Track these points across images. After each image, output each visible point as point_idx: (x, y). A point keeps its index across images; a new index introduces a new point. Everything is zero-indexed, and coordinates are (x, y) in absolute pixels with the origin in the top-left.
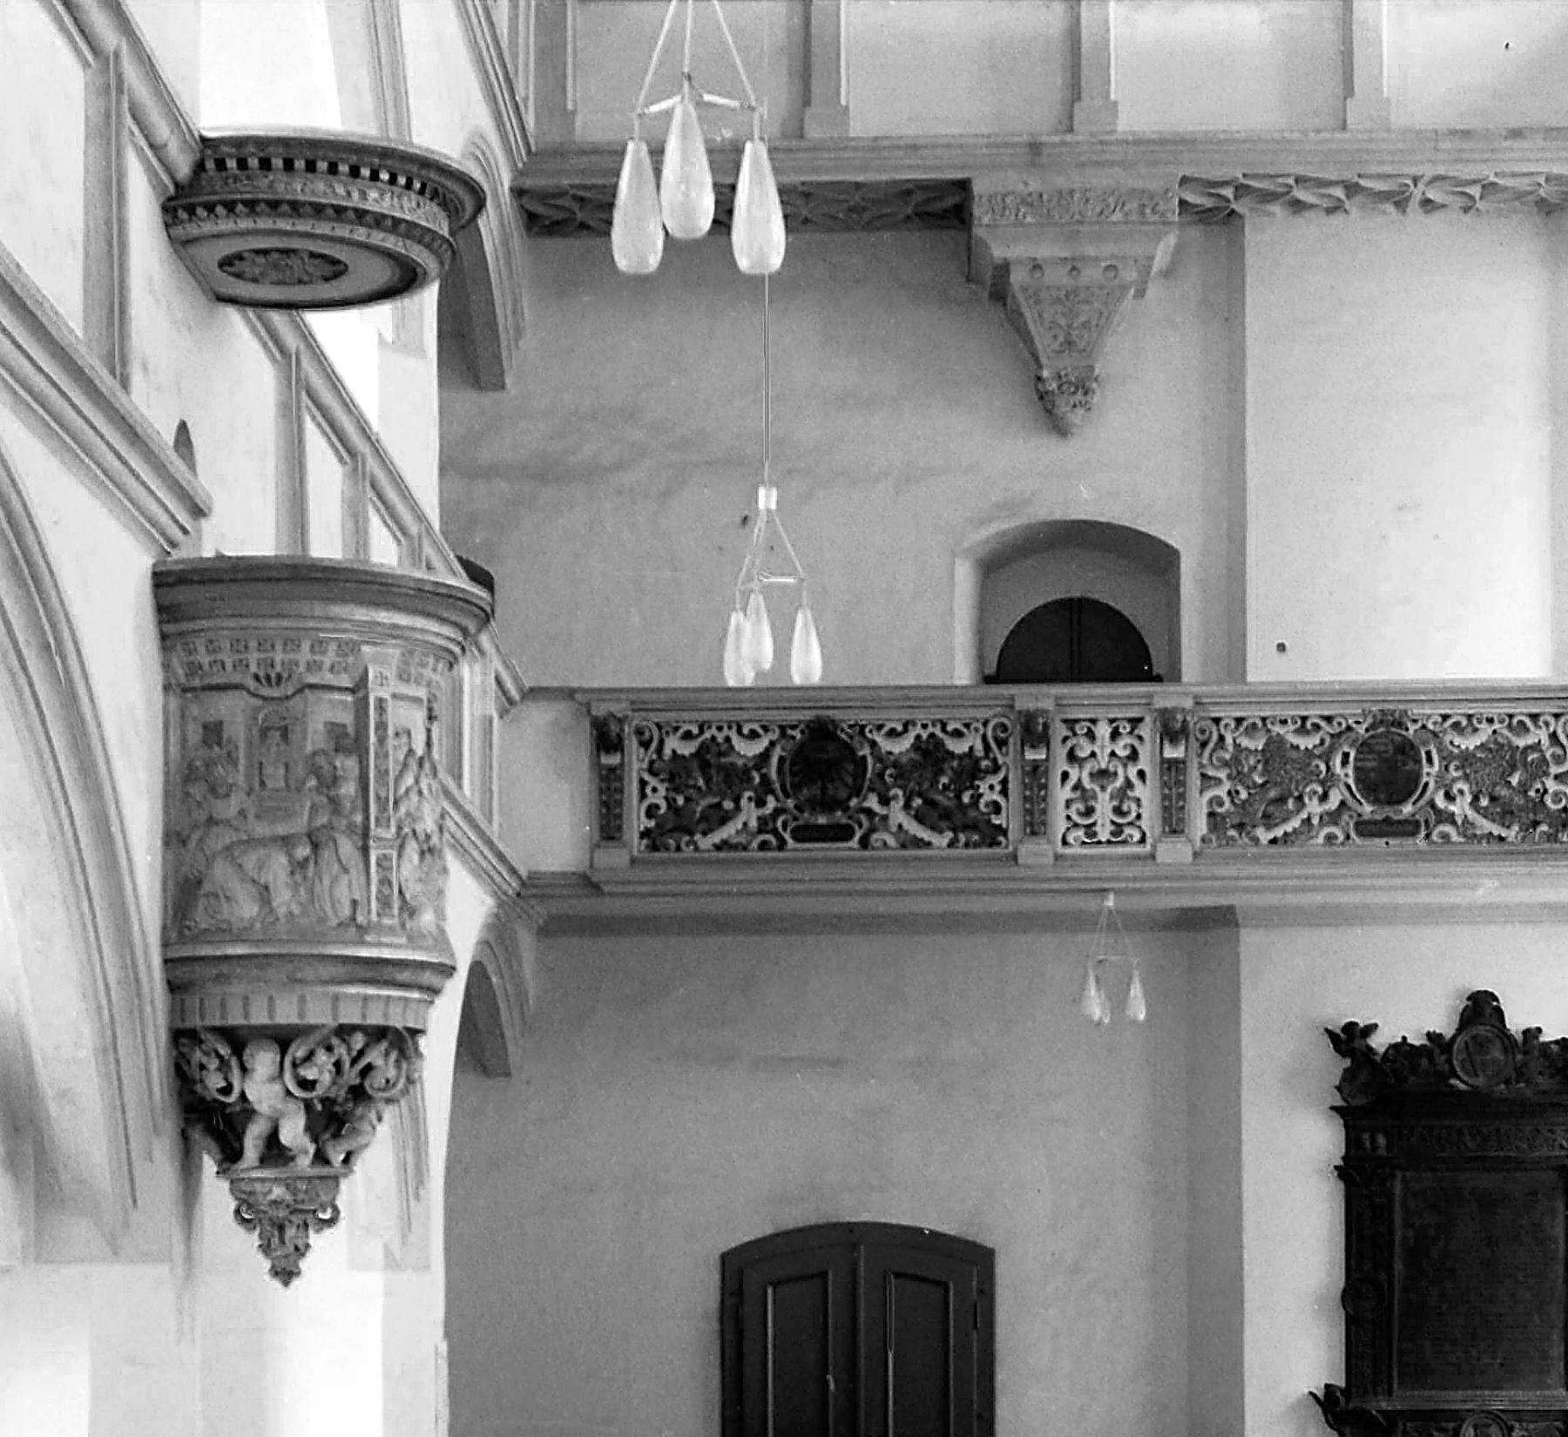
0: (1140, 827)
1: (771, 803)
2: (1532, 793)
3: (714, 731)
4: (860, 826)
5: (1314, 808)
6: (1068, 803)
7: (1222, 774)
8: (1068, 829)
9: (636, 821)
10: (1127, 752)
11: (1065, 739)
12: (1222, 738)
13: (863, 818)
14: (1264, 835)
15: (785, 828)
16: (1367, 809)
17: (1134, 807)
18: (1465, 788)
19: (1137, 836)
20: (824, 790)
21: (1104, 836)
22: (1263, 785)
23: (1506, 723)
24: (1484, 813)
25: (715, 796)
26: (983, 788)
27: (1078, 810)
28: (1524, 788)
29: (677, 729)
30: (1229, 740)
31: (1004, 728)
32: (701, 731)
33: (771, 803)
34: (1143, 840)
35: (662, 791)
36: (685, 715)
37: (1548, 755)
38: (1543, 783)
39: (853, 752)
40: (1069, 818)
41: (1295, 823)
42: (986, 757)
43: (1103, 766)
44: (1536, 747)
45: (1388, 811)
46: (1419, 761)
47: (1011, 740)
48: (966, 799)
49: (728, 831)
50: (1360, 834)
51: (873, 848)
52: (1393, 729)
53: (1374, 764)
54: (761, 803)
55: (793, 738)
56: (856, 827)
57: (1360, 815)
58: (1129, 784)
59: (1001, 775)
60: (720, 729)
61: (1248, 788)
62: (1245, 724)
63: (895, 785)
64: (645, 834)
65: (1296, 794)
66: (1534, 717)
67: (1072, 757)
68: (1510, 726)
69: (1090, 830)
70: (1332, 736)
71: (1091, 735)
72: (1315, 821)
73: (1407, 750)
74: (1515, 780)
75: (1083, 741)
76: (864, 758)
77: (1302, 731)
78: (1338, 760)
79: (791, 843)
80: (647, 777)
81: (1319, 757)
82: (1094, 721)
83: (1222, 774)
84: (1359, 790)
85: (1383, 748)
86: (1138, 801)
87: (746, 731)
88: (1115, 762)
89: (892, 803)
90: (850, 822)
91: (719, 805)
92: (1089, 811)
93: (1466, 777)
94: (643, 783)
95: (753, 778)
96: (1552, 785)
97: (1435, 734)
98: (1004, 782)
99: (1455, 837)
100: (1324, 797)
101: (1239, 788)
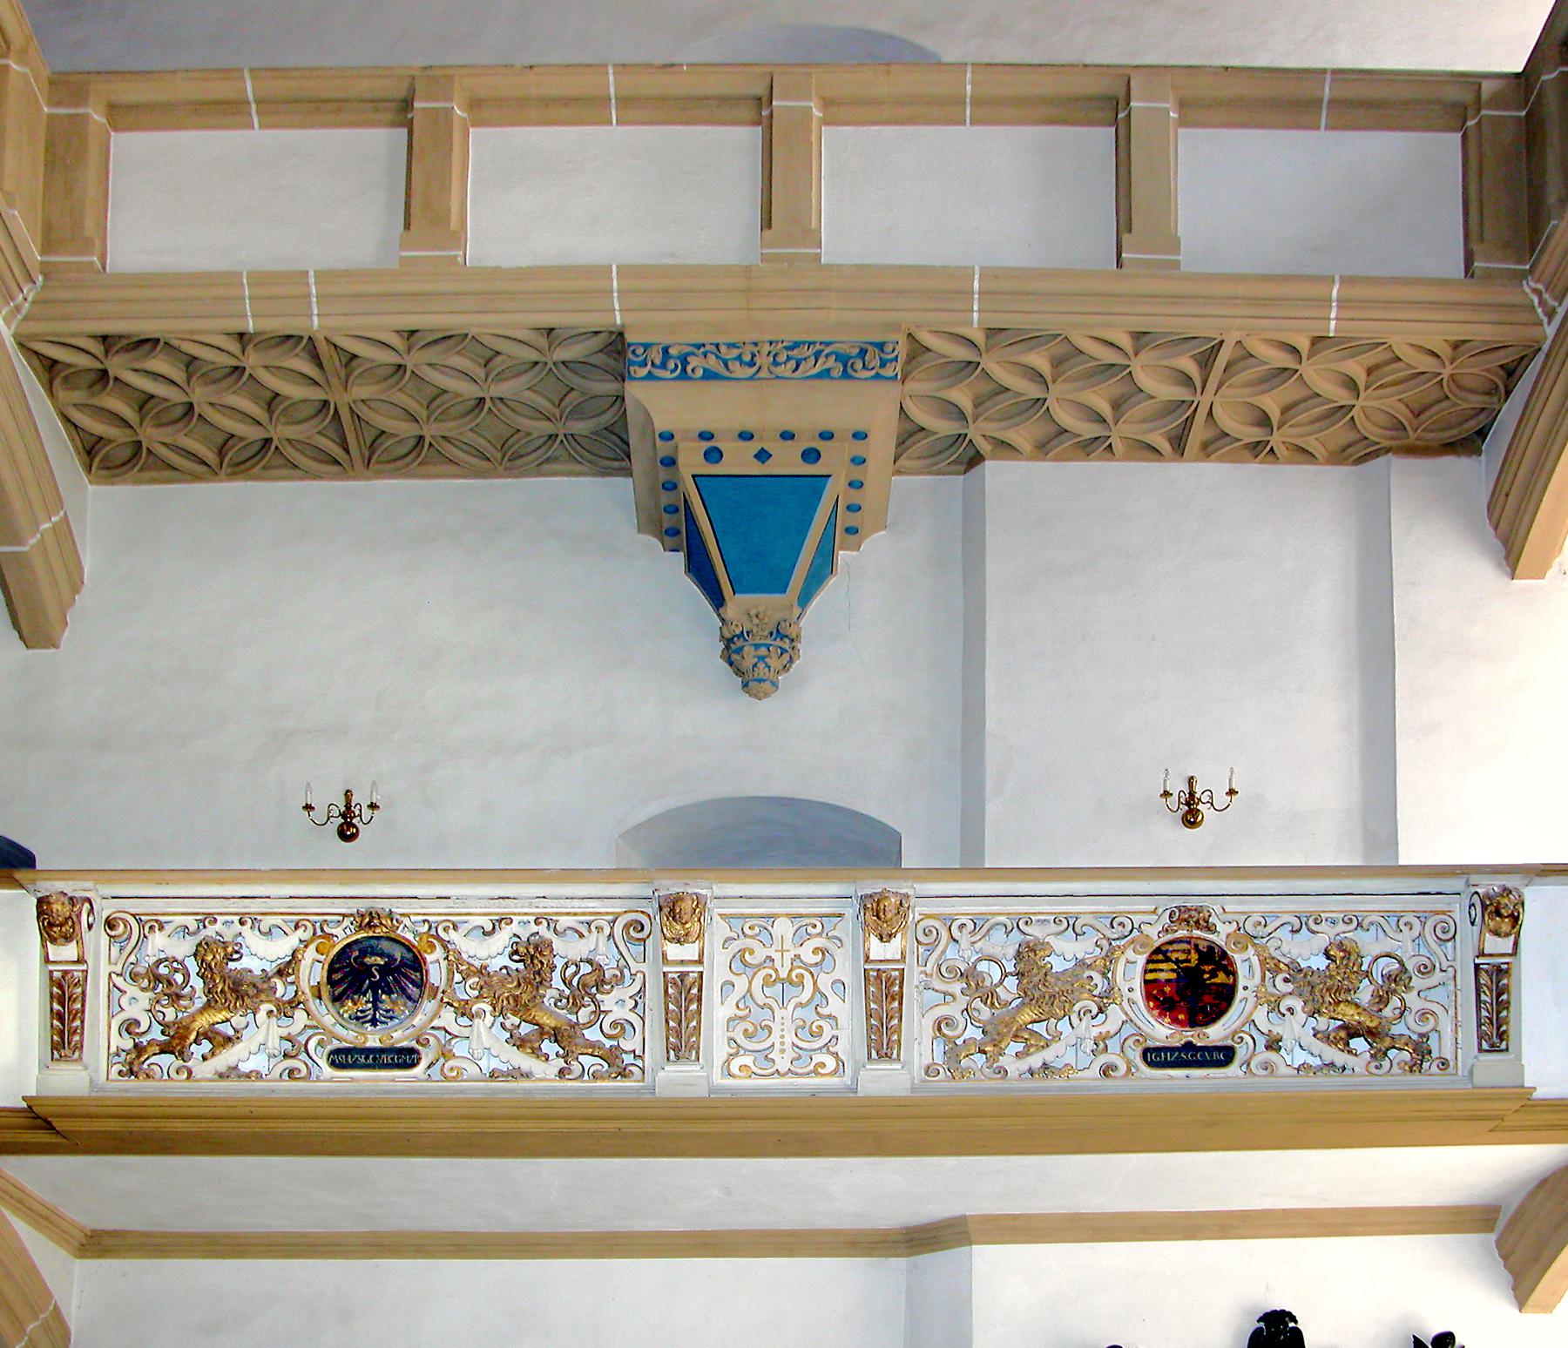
3: (218, 927)
8: (733, 1056)
20: (376, 1002)
27: (746, 1030)
35: (145, 999)
36: (179, 906)
38: (1402, 1000)
53: (1173, 976)
85: (1182, 957)
101: (978, 1003)
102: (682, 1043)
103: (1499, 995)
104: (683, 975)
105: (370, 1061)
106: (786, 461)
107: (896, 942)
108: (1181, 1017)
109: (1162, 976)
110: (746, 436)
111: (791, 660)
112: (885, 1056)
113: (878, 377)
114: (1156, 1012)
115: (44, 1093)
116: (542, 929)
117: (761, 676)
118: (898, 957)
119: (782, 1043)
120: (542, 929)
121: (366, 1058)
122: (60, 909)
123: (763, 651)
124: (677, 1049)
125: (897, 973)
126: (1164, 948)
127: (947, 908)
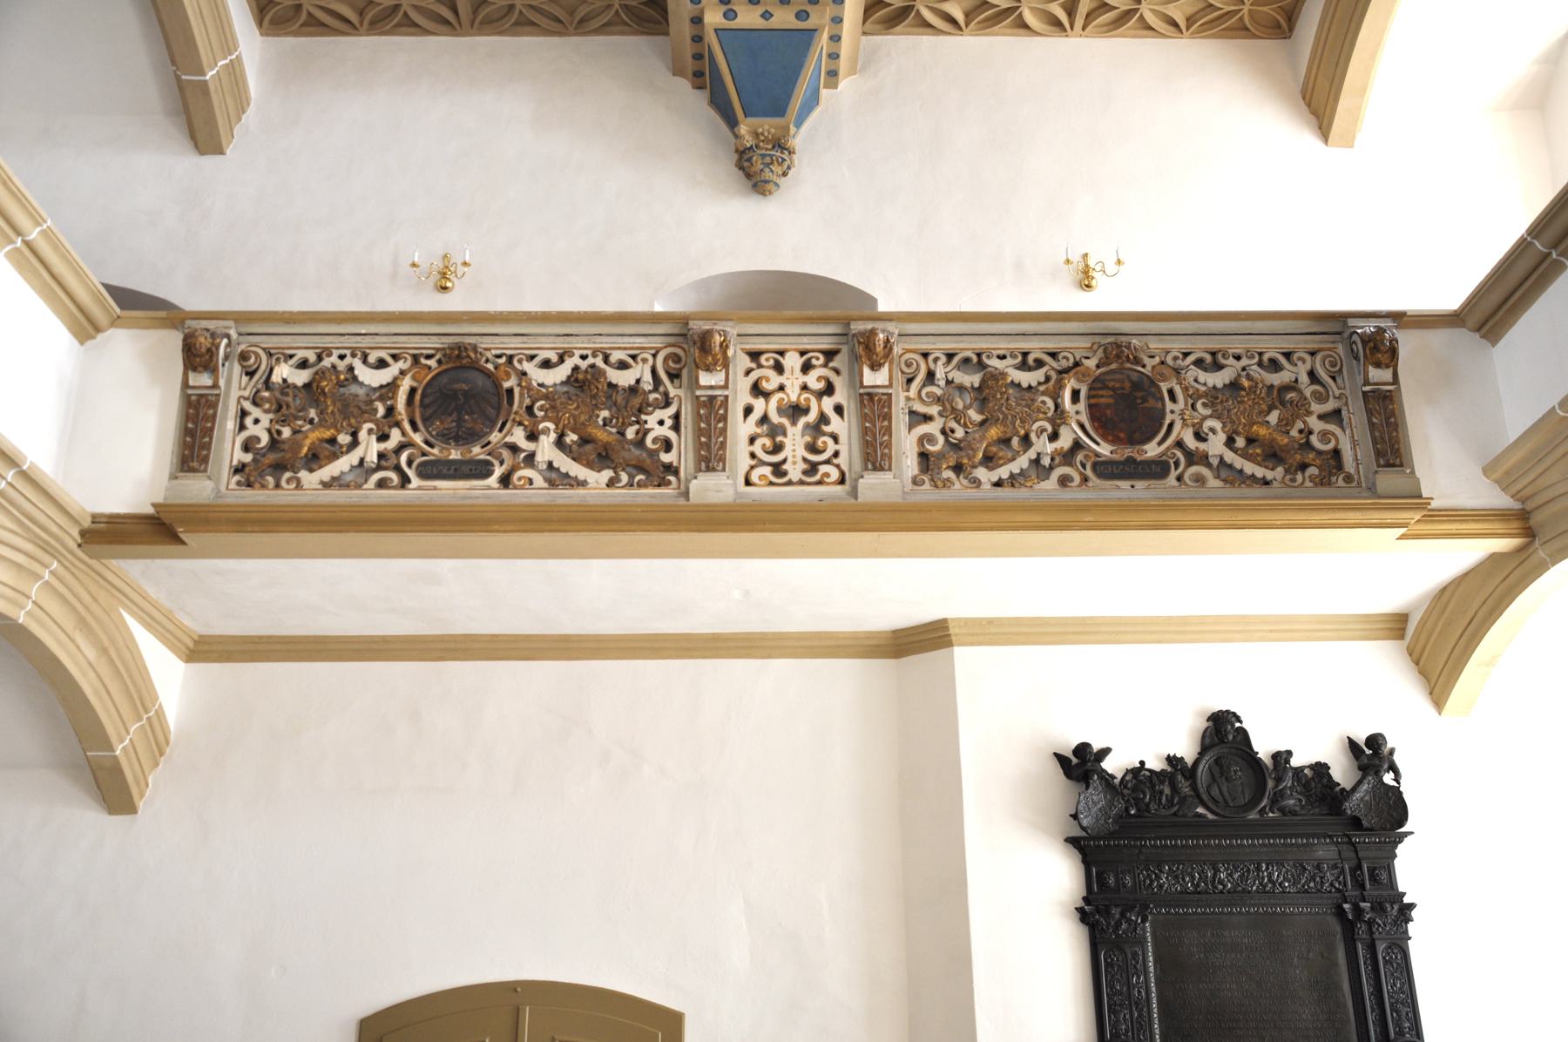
0: (838, 466)
1: (396, 437)
2: (1294, 433)
3: (334, 359)
4: (502, 463)
5: (1043, 446)
6: (752, 440)
7: (934, 410)
8: (752, 467)
9: (228, 449)
10: (821, 385)
11: (748, 373)
12: (931, 375)
13: (505, 453)
14: (981, 473)
15: (410, 463)
16: (1105, 449)
17: (830, 441)
18: (1217, 425)
20: (460, 420)
21: (795, 471)
22: (983, 423)
23: (1256, 360)
24: (1245, 455)
25: (328, 428)
26: (651, 420)
27: (764, 445)
28: (1285, 425)
29: (291, 356)
30: (940, 374)
31: (677, 359)
32: (320, 358)
33: (396, 437)
34: (842, 481)
35: (266, 420)
36: (301, 341)
37: (1308, 395)
38: (1304, 422)
39: (497, 385)
40: (753, 456)
41: (1023, 462)
42: (656, 389)
43: (794, 398)
44: (1293, 386)
45: (1128, 452)
46: (1162, 399)
47: (685, 373)
48: (630, 433)
49: (343, 464)
50: (1101, 476)
51: (515, 488)
52: (1128, 365)
53: (1111, 401)
54: (383, 438)
55: (430, 368)
56: (496, 463)
57: (1097, 455)
58: (823, 419)
59: (672, 410)
60: (342, 357)
61: (965, 426)
62: (956, 360)
63: (545, 419)
64: (239, 469)
65: (1022, 432)
66: (1288, 355)
67: (757, 390)
68: (1260, 364)
69: (778, 470)
70: (1060, 372)
71: (779, 368)
72: (1046, 461)
74: (1273, 418)
75: (771, 373)
76: (510, 391)
77: (1024, 366)
78: (1067, 395)
79: (415, 482)
80: (247, 405)
81: (1043, 393)
82: (782, 353)
83: (934, 410)
84: (1096, 429)
85: (1117, 385)
86: (835, 438)
87: (372, 359)
88: (805, 395)
89: (543, 438)
90: (488, 458)
92: (777, 448)
95: (376, 410)
96: (1314, 423)
97: (1177, 371)
98: (677, 417)
99: (1213, 483)
100: (1054, 437)
101: (953, 424)
102: (711, 457)
103: (1387, 419)
104: (712, 398)
105: (452, 472)
107: (885, 370)
108: (1122, 435)
109: (1103, 400)
111: (789, 168)
112: (878, 468)
114: (1101, 431)
115: (171, 501)
116: (599, 362)
117: (767, 178)
118: (887, 383)
119: (794, 456)
120: (599, 362)
121: (449, 470)
122: (203, 341)
124: (707, 460)
125: (885, 397)
126: (1102, 378)
127: (924, 345)
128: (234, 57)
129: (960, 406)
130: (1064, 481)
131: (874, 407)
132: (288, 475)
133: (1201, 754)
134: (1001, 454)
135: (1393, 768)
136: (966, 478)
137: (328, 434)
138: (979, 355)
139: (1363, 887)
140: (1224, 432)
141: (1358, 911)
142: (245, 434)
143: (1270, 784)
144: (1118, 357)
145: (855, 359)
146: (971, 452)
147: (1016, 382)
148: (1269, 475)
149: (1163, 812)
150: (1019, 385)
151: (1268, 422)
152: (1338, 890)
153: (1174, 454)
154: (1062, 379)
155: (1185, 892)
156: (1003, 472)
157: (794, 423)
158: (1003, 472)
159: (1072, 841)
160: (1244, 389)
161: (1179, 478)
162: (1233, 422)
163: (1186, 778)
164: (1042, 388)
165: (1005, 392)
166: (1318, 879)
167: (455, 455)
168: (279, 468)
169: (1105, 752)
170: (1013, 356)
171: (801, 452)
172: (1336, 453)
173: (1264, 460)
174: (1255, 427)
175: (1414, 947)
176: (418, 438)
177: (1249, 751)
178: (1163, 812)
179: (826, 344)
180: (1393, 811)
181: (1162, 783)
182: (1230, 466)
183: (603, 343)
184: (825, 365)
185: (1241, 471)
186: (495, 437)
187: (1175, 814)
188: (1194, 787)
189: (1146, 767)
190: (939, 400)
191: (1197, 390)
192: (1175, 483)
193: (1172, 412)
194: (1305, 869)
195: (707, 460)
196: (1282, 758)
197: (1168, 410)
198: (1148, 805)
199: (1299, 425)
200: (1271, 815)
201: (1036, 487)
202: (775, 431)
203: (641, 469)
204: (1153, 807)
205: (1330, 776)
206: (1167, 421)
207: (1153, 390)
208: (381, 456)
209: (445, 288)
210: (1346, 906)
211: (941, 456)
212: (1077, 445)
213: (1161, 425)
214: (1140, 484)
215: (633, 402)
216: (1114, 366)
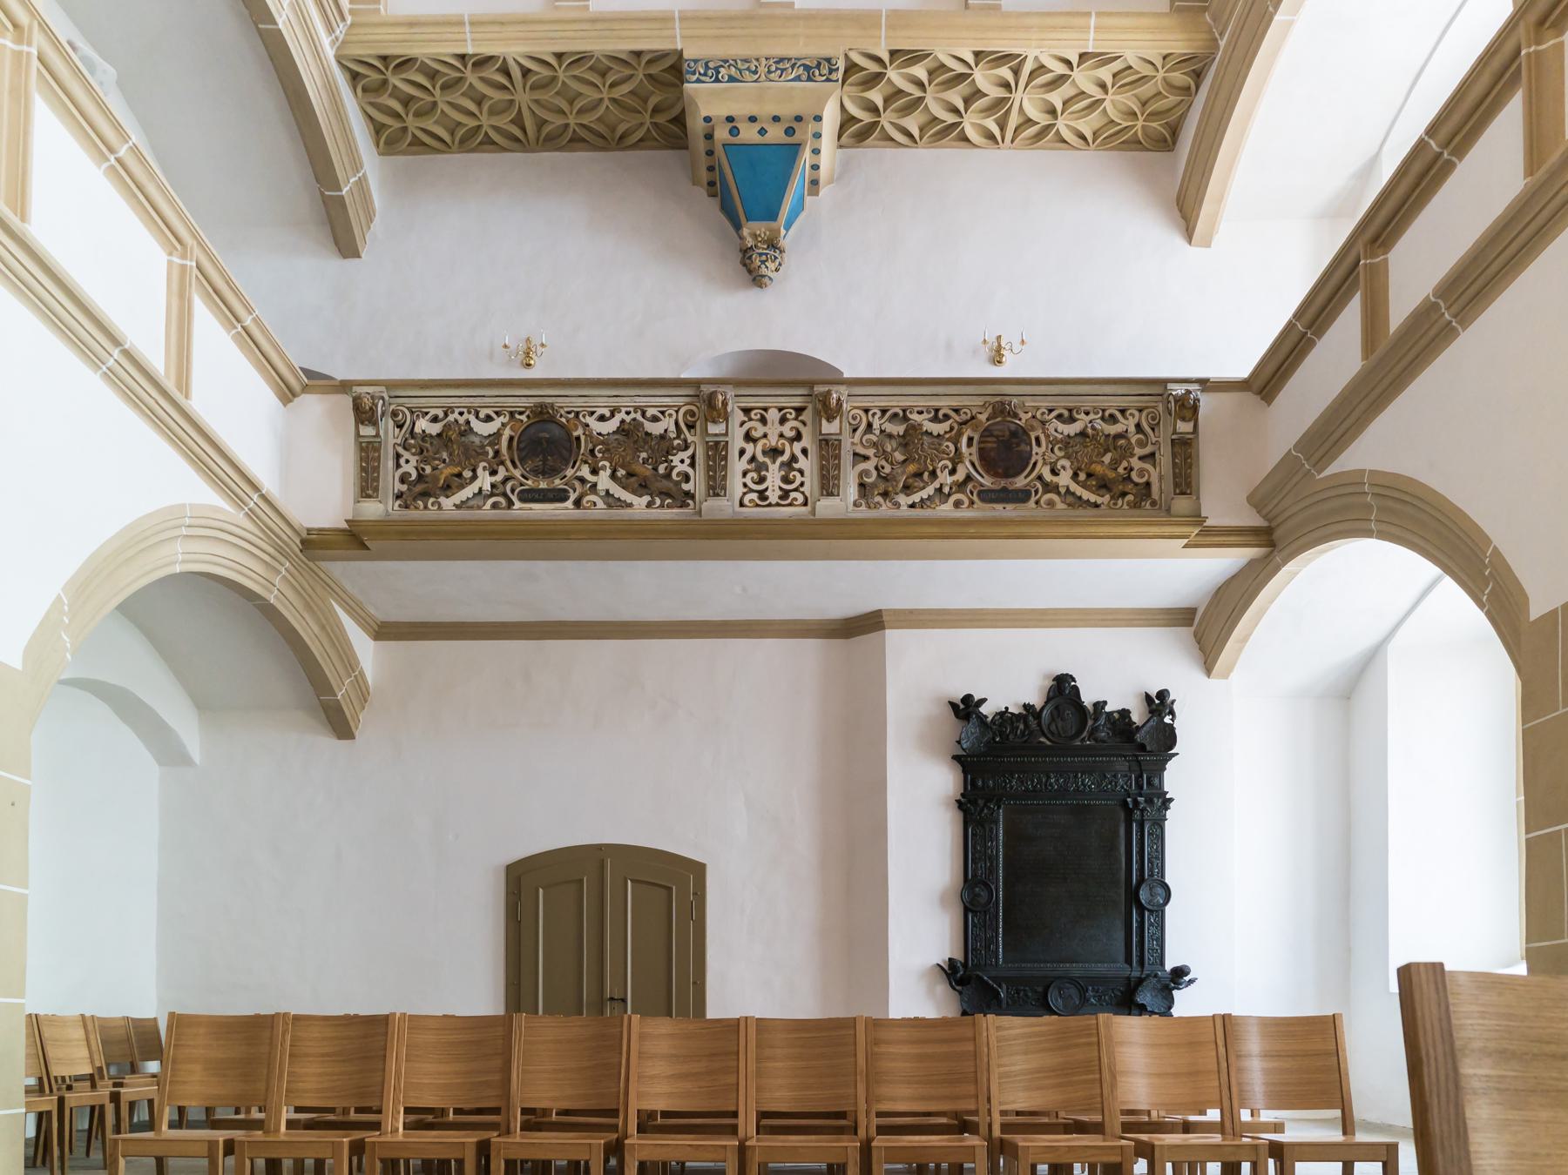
0: (803, 493)
1: (502, 473)
3: (456, 415)
4: (575, 491)
5: (945, 479)
6: (745, 474)
7: (871, 452)
8: (745, 494)
9: (390, 480)
10: (792, 434)
11: (742, 424)
12: (870, 425)
13: (577, 484)
14: (903, 500)
15: (513, 491)
16: (987, 482)
19: (801, 499)
20: (545, 461)
21: (773, 496)
22: (905, 461)
23: (1100, 415)
24: (1084, 486)
25: (456, 466)
26: (676, 460)
27: (752, 478)
28: (1114, 465)
29: (427, 413)
30: (876, 425)
31: (692, 414)
32: (446, 415)
33: (502, 473)
34: (805, 504)
35: (414, 460)
37: (1133, 441)
38: (1128, 462)
39: (569, 434)
40: (745, 485)
41: (930, 490)
42: (678, 437)
43: (774, 444)
45: (1003, 483)
47: (698, 424)
48: (662, 469)
50: (983, 500)
51: (585, 509)
52: (1009, 419)
53: (995, 445)
55: (522, 421)
56: (571, 491)
57: (982, 485)
58: (794, 458)
59: (690, 452)
60: (461, 414)
61: (892, 464)
62: (888, 414)
63: (603, 459)
64: (399, 496)
65: (931, 468)
66: (1123, 412)
67: (748, 437)
68: (1103, 418)
69: (762, 495)
70: (961, 424)
71: (763, 421)
72: (946, 490)
73: (1020, 435)
74: (1107, 458)
75: (758, 425)
76: (578, 438)
77: (935, 419)
78: (964, 440)
79: (518, 504)
80: (400, 450)
81: (948, 440)
82: (766, 409)
83: (871, 452)
84: (983, 466)
85: (1000, 433)
86: (801, 472)
87: (482, 415)
88: (782, 441)
89: (601, 472)
90: (566, 487)
91: (459, 475)
92: (762, 480)
93: (1067, 457)
94: (398, 456)
96: (1135, 463)
97: (1043, 423)
98: (693, 457)
99: (1060, 506)
100: (953, 472)
101: (883, 463)
102: (716, 487)
103: (1185, 460)
104: (717, 443)
105: (541, 497)
106: (775, 134)
108: (1000, 471)
109: (990, 445)
110: (753, 119)
112: (830, 494)
113: (828, 80)
116: (639, 416)
118: (838, 432)
119: (773, 486)
120: (639, 416)
121: (539, 495)
122: (367, 402)
123: (764, 258)
124: (713, 488)
125: (836, 442)
128: (361, 174)
129: (889, 449)
130: (957, 504)
131: (828, 447)
132: (432, 500)
133: (1046, 703)
134: (916, 484)
135: (1172, 713)
136: (890, 501)
137: (456, 470)
138: (904, 411)
139: (1142, 788)
140: (1072, 469)
141: (1136, 803)
142: (401, 471)
143: (1090, 723)
144: (1002, 412)
145: (817, 415)
146: (895, 483)
147: (929, 431)
148: (1099, 500)
149: (1017, 740)
150: (931, 434)
151: (1103, 462)
152: (1125, 790)
153: (1035, 485)
154: (962, 428)
155: (1027, 790)
156: (916, 498)
157: (774, 462)
158: (916, 498)
159: (956, 758)
160: (1089, 437)
161: (1037, 502)
162: (1078, 461)
163: (1035, 719)
164: (947, 436)
165: (921, 439)
166: (1113, 784)
167: (543, 485)
168: (425, 495)
169: (983, 701)
170: (929, 412)
171: (779, 483)
172: (1148, 484)
173: (1097, 490)
174: (1093, 466)
175: (1168, 825)
176: (517, 473)
177: (1078, 700)
178: (1017, 740)
179: (797, 402)
180: (1167, 738)
181: (1018, 721)
182: (1073, 494)
183: (641, 402)
184: (796, 419)
185: (1080, 498)
186: (570, 472)
187: (1025, 742)
188: (1039, 724)
189: (1010, 711)
190: (875, 445)
191: (1056, 437)
192: (1034, 506)
193: (1037, 454)
194: (1105, 776)
195: (713, 488)
196: (1099, 706)
197: (1034, 453)
198: (1008, 736)
199: (1125, 464)
200: (1088, 743)
201: (937, 508)
202: (761, 467)
203: (669, 495)
204: (1011, 737)
205: (1130, 718)
206: (1032, 462)
207: (1025, 437)
208: (493, 486)
209: (529, 365)
210: (1129, 800)
211: (874, 485)
212: (969, 478)
213: (1028, 464)
214: (1010, 507)
215: (663, 447)
216: (999, 419)
